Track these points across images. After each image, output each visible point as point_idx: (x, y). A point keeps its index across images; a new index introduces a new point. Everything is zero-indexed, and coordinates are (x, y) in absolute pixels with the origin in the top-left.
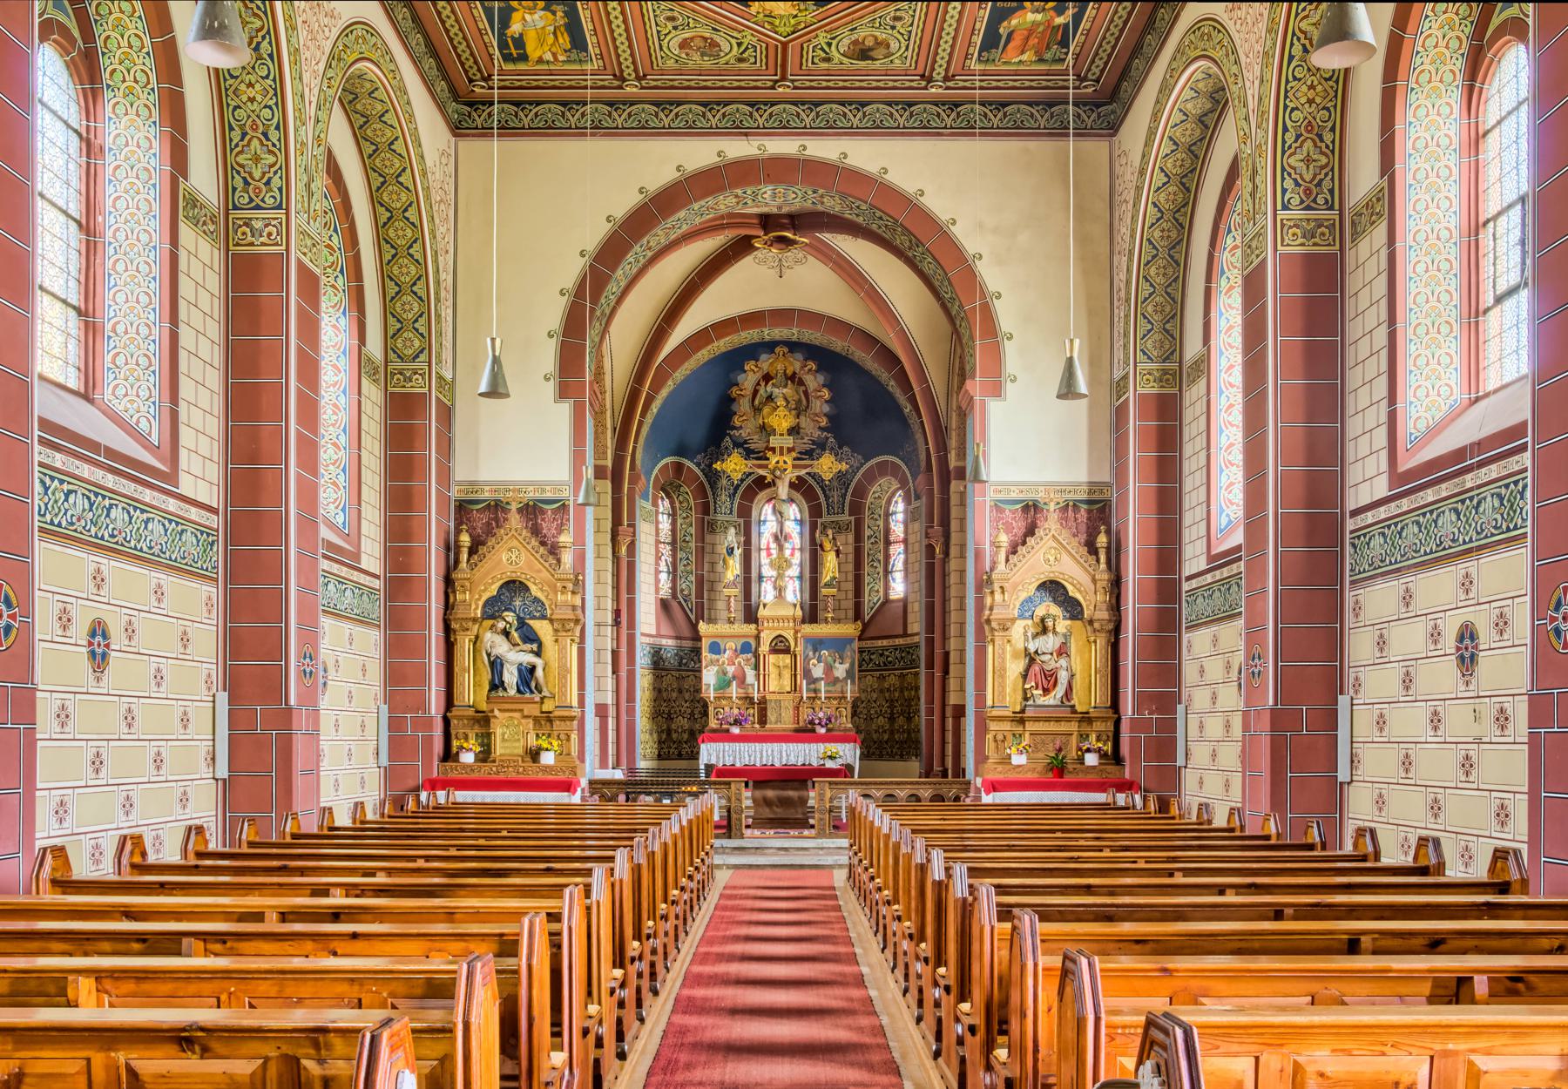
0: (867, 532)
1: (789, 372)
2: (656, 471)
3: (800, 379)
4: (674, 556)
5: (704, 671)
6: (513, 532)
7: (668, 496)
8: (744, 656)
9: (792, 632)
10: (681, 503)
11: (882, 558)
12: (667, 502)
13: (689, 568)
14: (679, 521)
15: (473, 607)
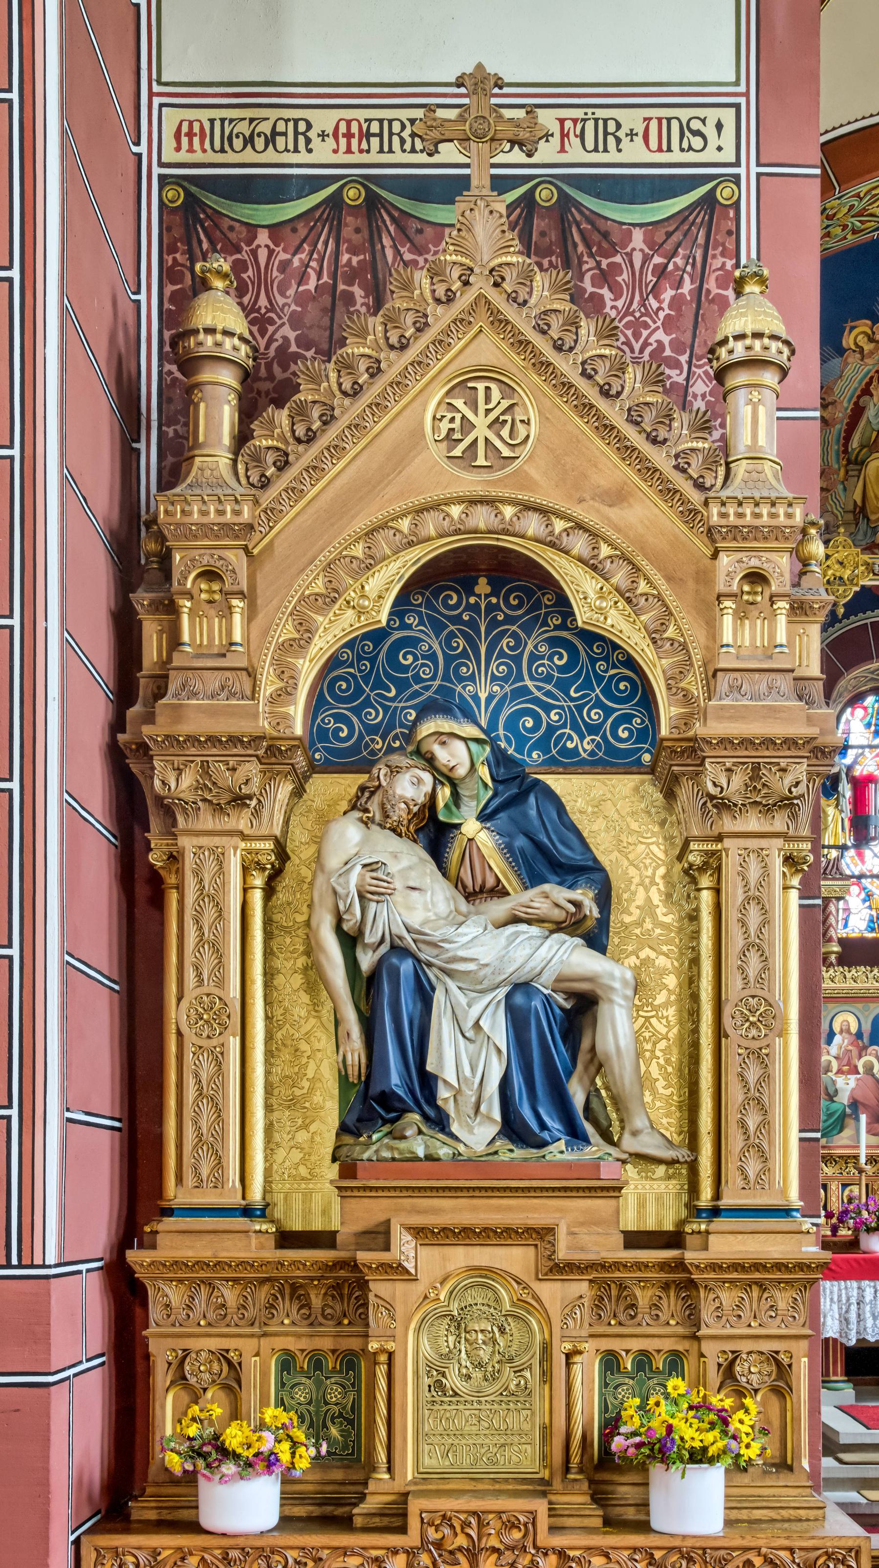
6: (481, 285)
15: (268, 685)
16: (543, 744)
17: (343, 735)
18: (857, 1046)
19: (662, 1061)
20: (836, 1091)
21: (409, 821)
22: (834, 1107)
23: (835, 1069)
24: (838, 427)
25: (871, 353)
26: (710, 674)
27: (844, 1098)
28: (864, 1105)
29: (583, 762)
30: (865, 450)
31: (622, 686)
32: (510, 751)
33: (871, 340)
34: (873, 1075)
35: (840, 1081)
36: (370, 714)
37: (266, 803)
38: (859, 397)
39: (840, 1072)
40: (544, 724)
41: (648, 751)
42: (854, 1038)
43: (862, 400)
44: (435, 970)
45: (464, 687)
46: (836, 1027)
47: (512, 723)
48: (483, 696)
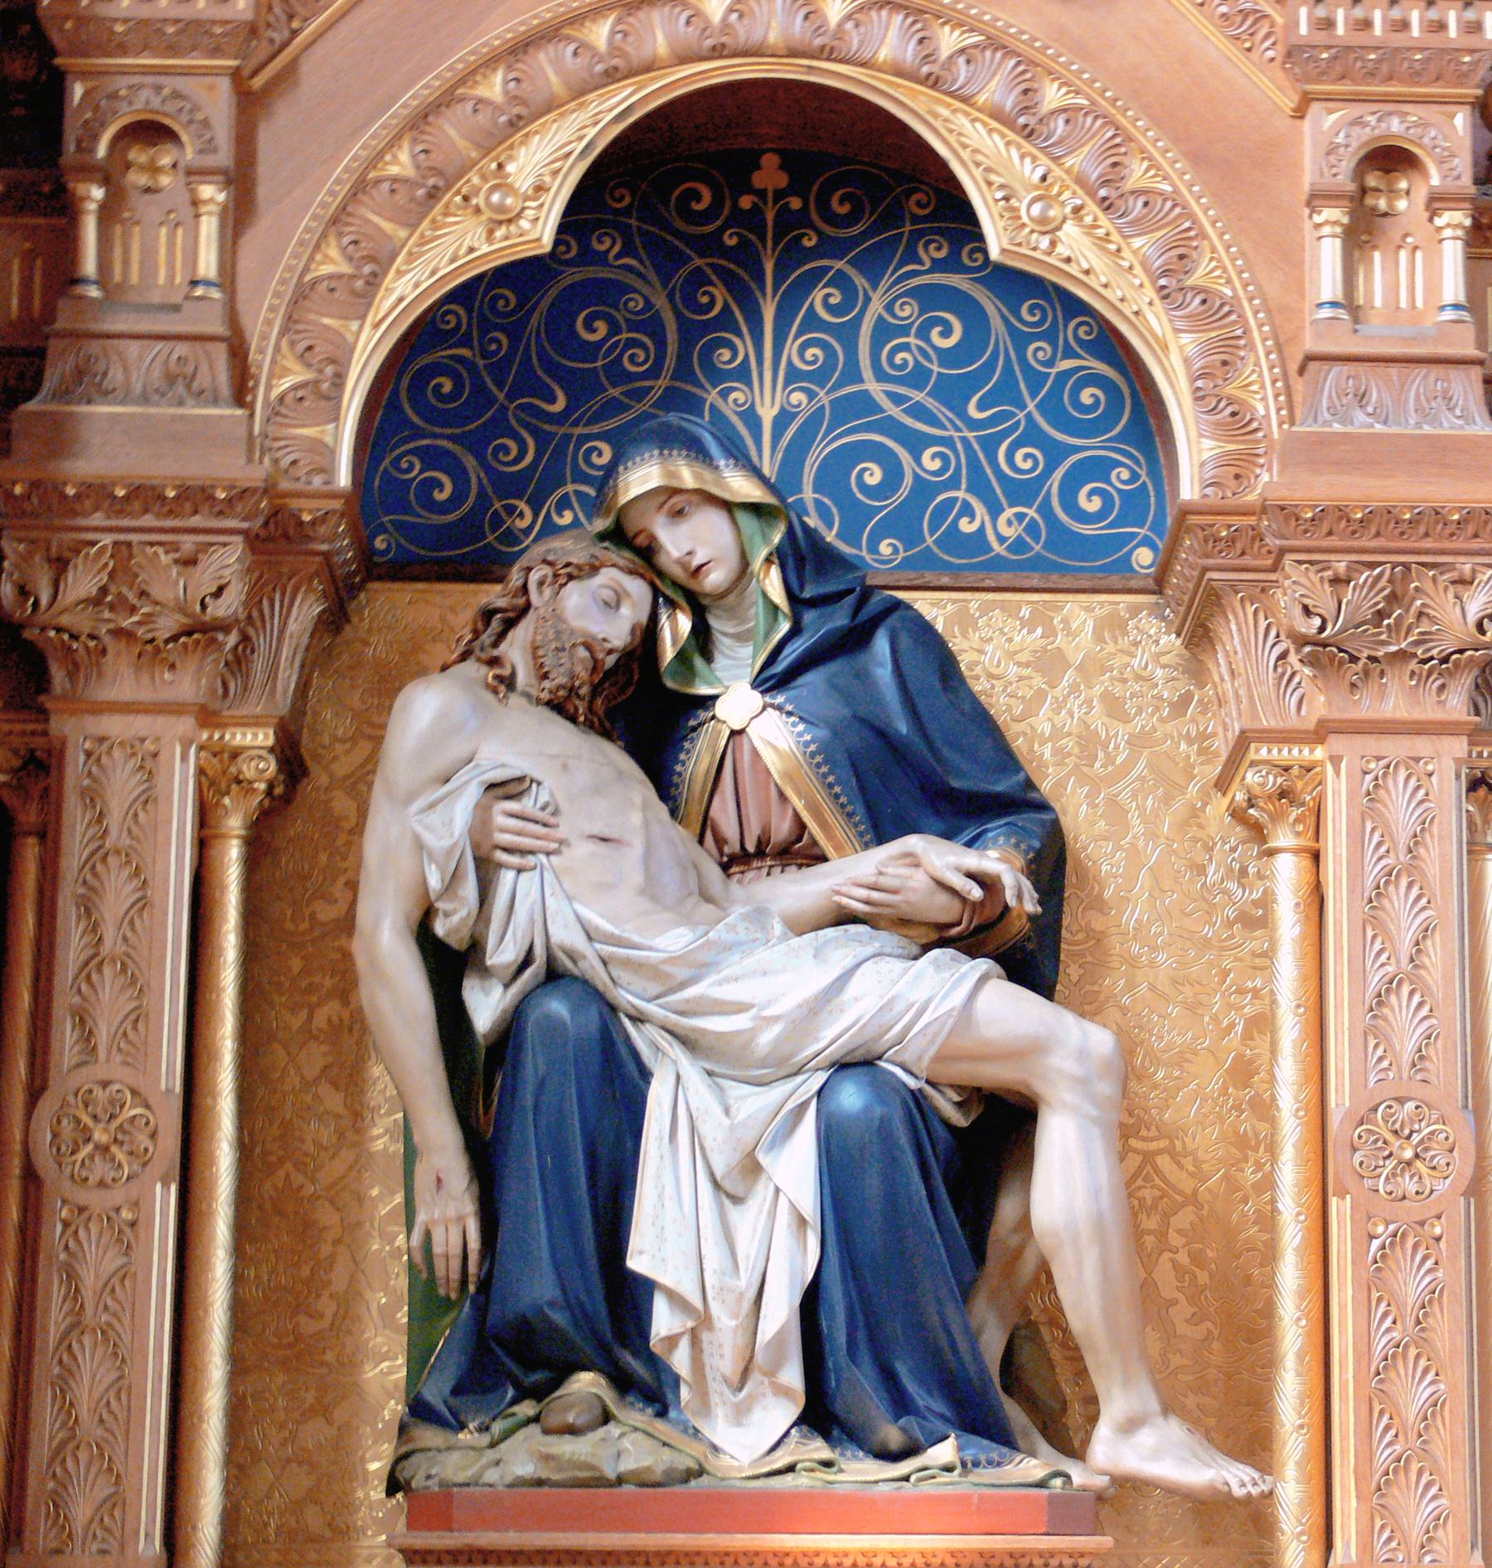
16: (903, 525)
17: (441, 496)
19: (1183, 1258)
21: (596, 690)
26: (1293, 367)
29: (998, 563)
31: (1086, 397)
32: (830, 537)
36: (507, 450)
37: (262, 643)
40: (908, 480)
41: (1147, 542)
44: (649, 1029)
45: (724, 394)
47: (833, 475)
48: (767, 413)
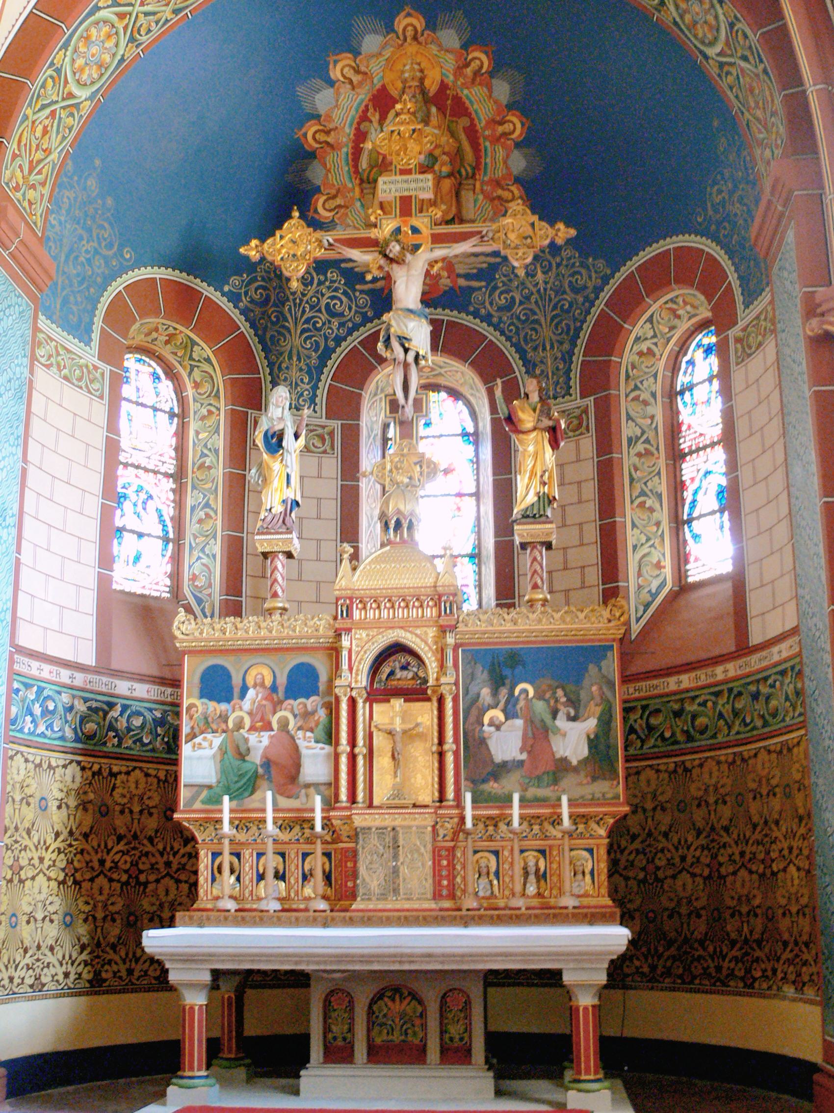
0: (627, 430)
1: (432, 87)
2: (118, 286)
3: (457, 100)
4: (179, 504)
5: (186, 750)
7: (171, 374)
8: (296, 704)
9: (432, 632)
10: (197, 385)
11: (663, 489)
12: (166, 387)
13: (208, 526)
14: (193, 426)
18: (272, 700)
20: (248, 749)
22: (246, 766)
23: (247, 726)
24: (344, 150)
25: (360, 83)
27: (256, 758)
28: (276, 764)
30: (375, 170)
33: (357, 71)
34: (288, 732)
35: (253, 738)
38: (359, 124)
39: (252, 728)
42: (267, 692)
43: (362, 127)
46: (250, 681)
